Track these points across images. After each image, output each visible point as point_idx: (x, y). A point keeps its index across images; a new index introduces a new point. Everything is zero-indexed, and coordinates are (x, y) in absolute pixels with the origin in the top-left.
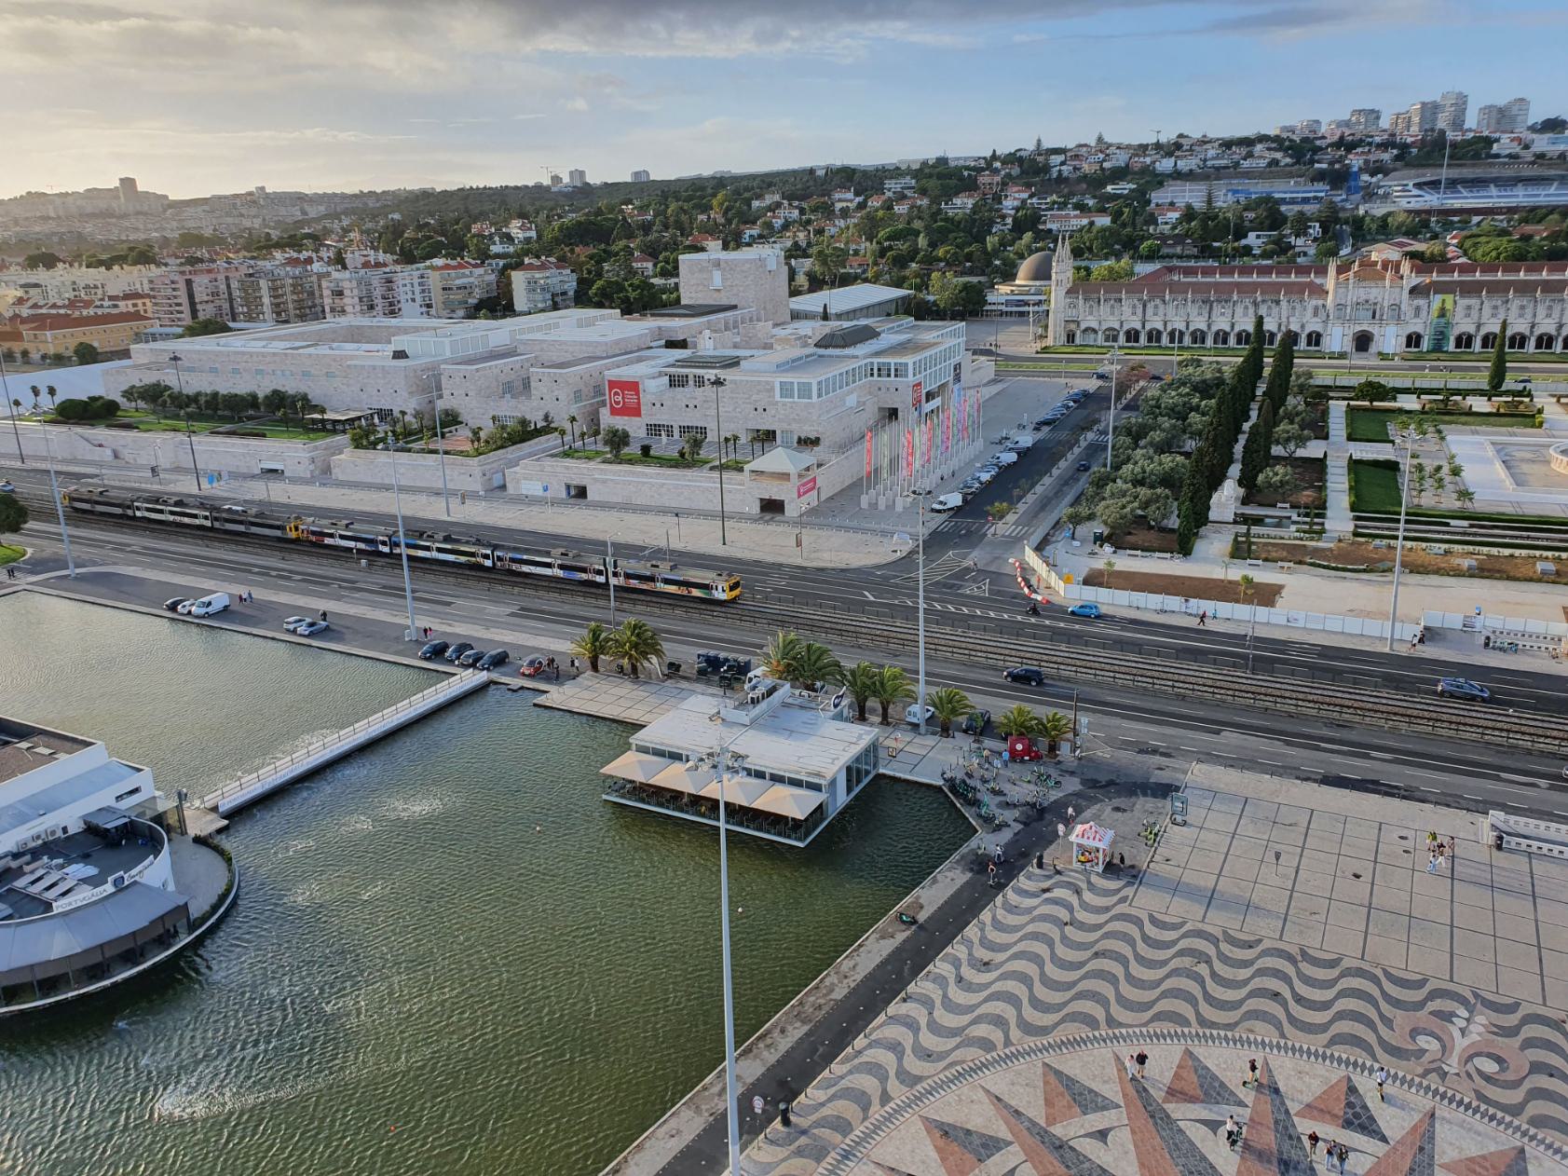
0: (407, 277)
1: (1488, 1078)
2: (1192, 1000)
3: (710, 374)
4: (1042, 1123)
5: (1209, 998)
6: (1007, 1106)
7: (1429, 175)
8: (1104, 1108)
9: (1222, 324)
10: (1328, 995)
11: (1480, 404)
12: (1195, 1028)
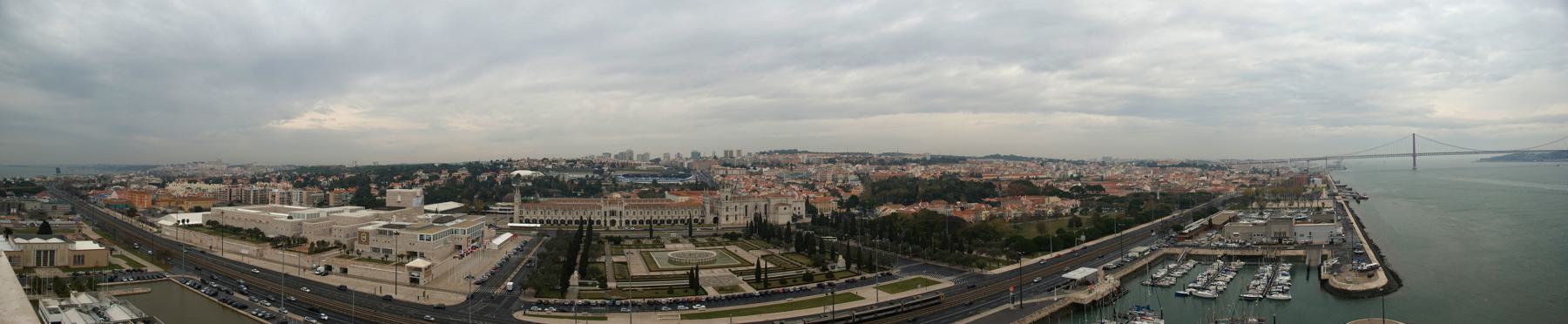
0: (296, 193)
3: (394, 231)
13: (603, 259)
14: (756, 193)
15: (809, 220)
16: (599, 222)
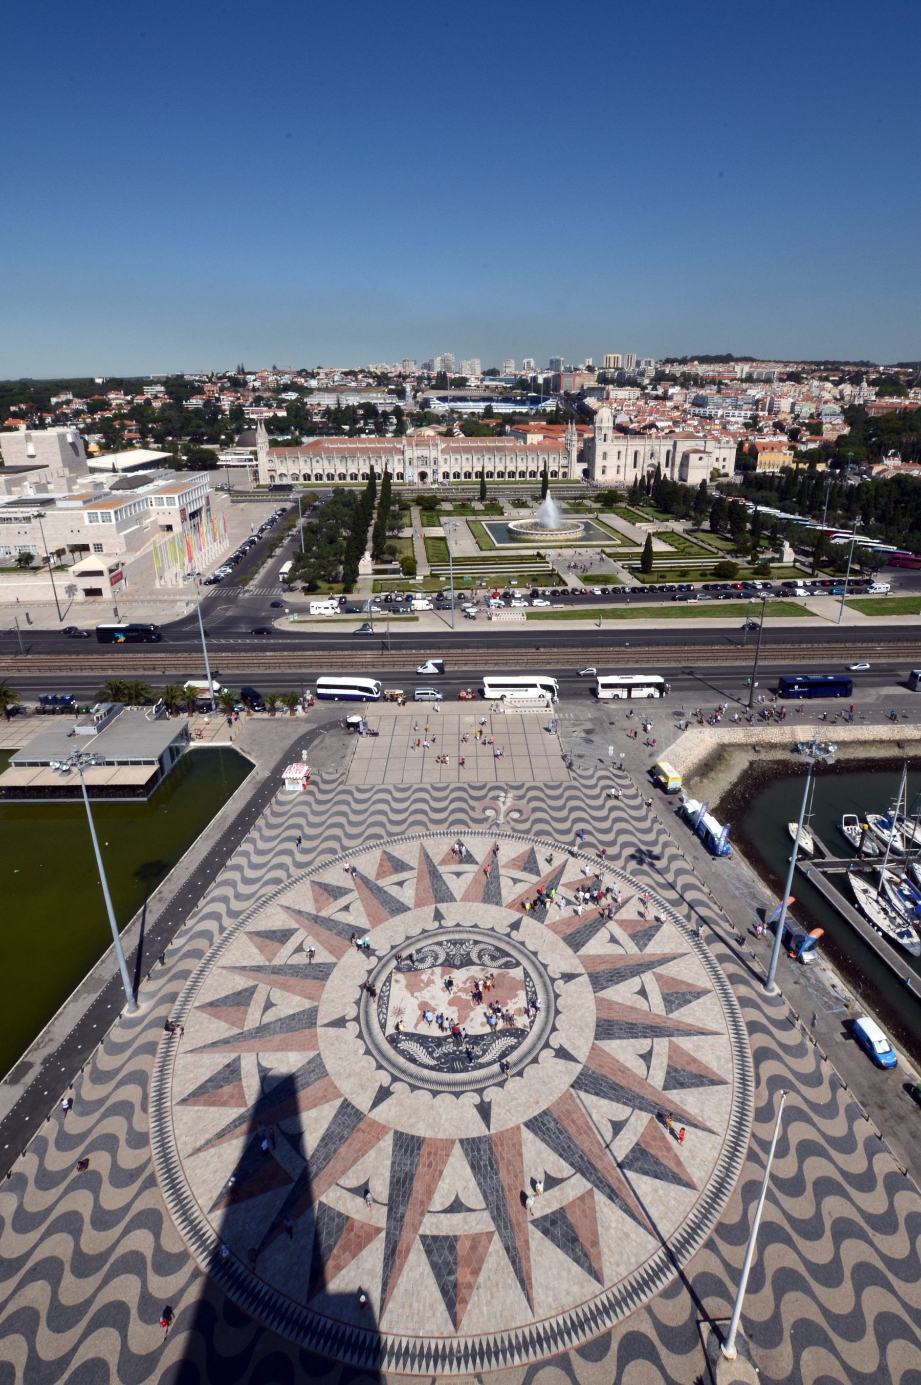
1: (515, 820)
2: (382, 825)
4: (314, 912)
5: (392, 822)
6: (294, 910)
7: (442, 393)
8: (346, 893)
9: (353, 469)
10: (446, 803)
11: (478, 506)
12: (386, 838)
13: (407, 532)
14: (654, 430)
15: (739, 480)
16: (401, 476)
